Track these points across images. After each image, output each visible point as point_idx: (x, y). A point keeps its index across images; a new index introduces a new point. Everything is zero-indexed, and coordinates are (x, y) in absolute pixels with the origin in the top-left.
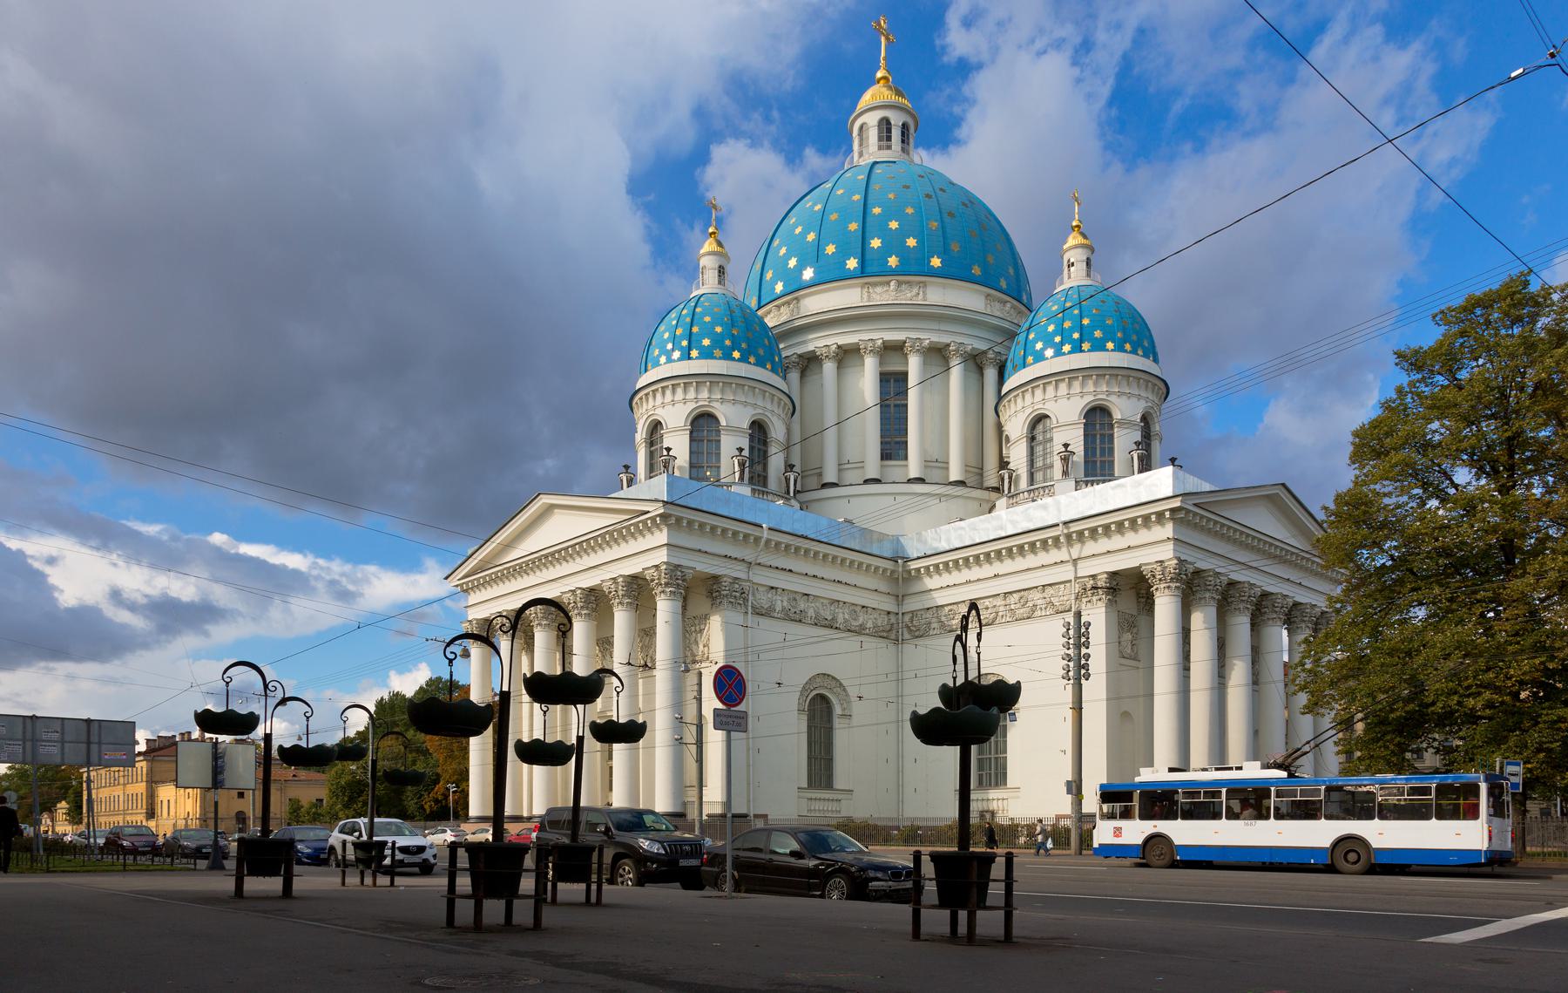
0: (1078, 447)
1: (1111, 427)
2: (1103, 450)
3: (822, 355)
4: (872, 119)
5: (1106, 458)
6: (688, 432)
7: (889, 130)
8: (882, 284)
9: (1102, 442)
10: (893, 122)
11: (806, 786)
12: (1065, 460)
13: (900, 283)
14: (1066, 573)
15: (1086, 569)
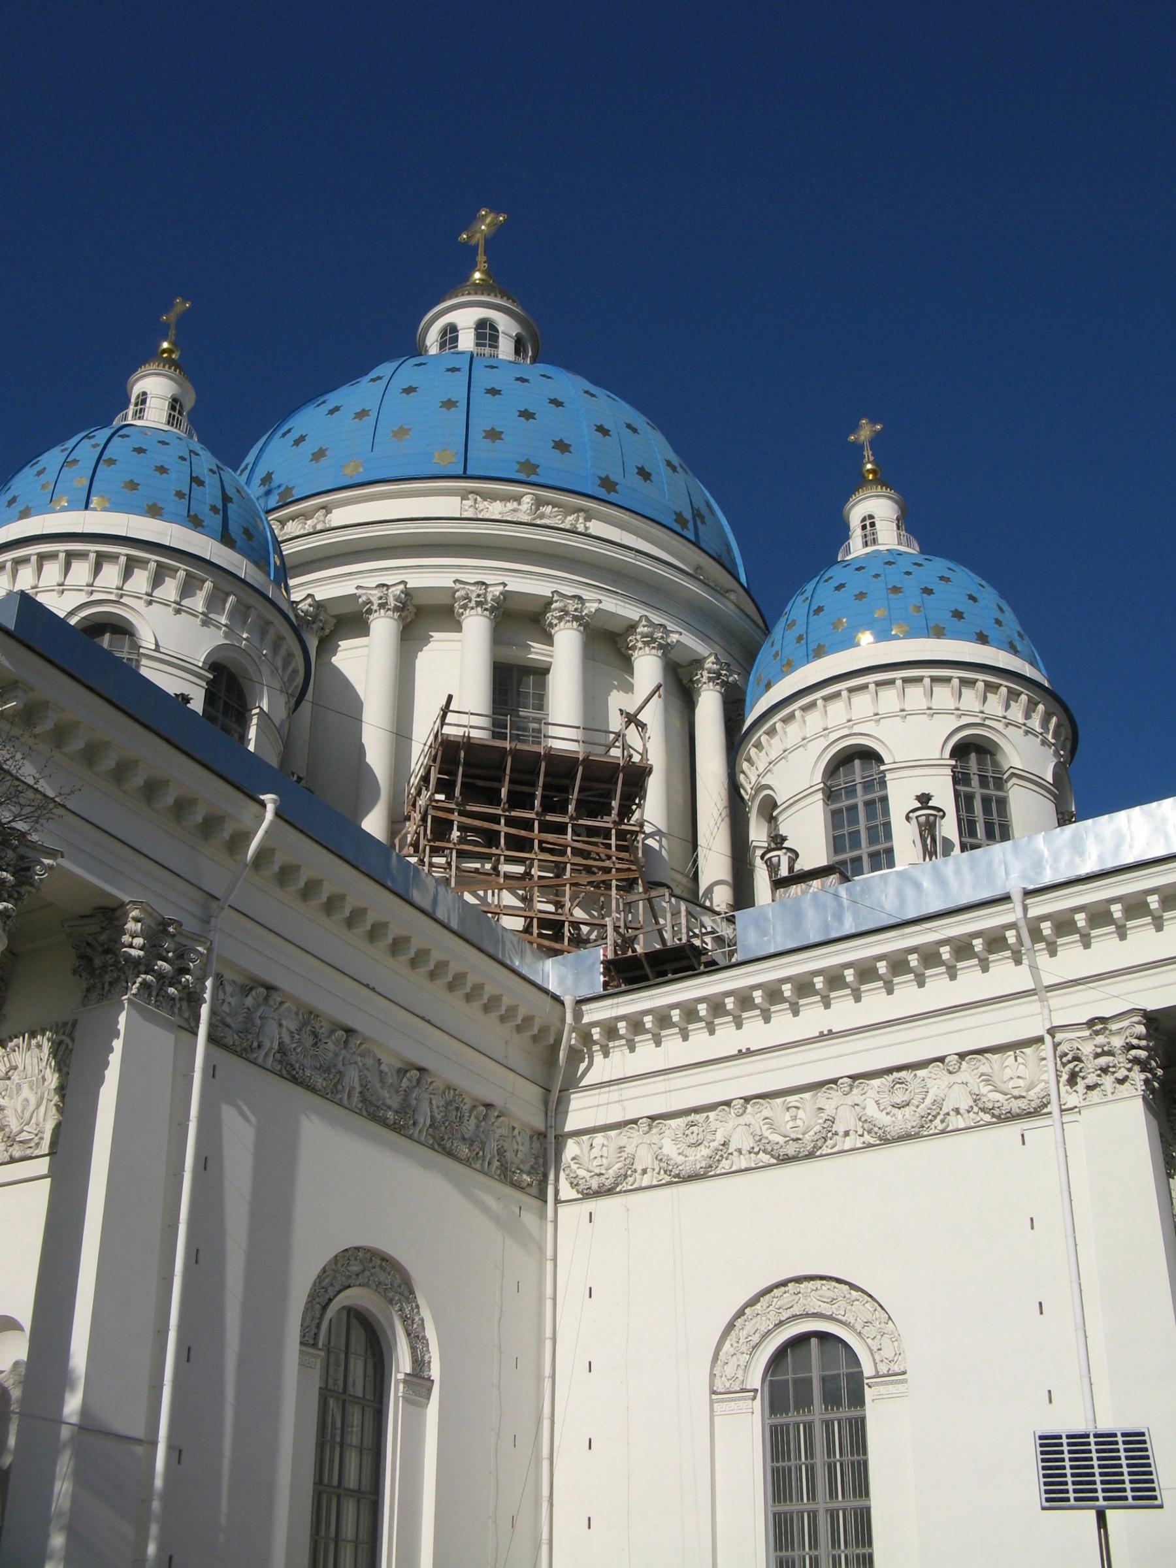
1: (1000, 784)
9: (987, 810)
12: (928, 829)
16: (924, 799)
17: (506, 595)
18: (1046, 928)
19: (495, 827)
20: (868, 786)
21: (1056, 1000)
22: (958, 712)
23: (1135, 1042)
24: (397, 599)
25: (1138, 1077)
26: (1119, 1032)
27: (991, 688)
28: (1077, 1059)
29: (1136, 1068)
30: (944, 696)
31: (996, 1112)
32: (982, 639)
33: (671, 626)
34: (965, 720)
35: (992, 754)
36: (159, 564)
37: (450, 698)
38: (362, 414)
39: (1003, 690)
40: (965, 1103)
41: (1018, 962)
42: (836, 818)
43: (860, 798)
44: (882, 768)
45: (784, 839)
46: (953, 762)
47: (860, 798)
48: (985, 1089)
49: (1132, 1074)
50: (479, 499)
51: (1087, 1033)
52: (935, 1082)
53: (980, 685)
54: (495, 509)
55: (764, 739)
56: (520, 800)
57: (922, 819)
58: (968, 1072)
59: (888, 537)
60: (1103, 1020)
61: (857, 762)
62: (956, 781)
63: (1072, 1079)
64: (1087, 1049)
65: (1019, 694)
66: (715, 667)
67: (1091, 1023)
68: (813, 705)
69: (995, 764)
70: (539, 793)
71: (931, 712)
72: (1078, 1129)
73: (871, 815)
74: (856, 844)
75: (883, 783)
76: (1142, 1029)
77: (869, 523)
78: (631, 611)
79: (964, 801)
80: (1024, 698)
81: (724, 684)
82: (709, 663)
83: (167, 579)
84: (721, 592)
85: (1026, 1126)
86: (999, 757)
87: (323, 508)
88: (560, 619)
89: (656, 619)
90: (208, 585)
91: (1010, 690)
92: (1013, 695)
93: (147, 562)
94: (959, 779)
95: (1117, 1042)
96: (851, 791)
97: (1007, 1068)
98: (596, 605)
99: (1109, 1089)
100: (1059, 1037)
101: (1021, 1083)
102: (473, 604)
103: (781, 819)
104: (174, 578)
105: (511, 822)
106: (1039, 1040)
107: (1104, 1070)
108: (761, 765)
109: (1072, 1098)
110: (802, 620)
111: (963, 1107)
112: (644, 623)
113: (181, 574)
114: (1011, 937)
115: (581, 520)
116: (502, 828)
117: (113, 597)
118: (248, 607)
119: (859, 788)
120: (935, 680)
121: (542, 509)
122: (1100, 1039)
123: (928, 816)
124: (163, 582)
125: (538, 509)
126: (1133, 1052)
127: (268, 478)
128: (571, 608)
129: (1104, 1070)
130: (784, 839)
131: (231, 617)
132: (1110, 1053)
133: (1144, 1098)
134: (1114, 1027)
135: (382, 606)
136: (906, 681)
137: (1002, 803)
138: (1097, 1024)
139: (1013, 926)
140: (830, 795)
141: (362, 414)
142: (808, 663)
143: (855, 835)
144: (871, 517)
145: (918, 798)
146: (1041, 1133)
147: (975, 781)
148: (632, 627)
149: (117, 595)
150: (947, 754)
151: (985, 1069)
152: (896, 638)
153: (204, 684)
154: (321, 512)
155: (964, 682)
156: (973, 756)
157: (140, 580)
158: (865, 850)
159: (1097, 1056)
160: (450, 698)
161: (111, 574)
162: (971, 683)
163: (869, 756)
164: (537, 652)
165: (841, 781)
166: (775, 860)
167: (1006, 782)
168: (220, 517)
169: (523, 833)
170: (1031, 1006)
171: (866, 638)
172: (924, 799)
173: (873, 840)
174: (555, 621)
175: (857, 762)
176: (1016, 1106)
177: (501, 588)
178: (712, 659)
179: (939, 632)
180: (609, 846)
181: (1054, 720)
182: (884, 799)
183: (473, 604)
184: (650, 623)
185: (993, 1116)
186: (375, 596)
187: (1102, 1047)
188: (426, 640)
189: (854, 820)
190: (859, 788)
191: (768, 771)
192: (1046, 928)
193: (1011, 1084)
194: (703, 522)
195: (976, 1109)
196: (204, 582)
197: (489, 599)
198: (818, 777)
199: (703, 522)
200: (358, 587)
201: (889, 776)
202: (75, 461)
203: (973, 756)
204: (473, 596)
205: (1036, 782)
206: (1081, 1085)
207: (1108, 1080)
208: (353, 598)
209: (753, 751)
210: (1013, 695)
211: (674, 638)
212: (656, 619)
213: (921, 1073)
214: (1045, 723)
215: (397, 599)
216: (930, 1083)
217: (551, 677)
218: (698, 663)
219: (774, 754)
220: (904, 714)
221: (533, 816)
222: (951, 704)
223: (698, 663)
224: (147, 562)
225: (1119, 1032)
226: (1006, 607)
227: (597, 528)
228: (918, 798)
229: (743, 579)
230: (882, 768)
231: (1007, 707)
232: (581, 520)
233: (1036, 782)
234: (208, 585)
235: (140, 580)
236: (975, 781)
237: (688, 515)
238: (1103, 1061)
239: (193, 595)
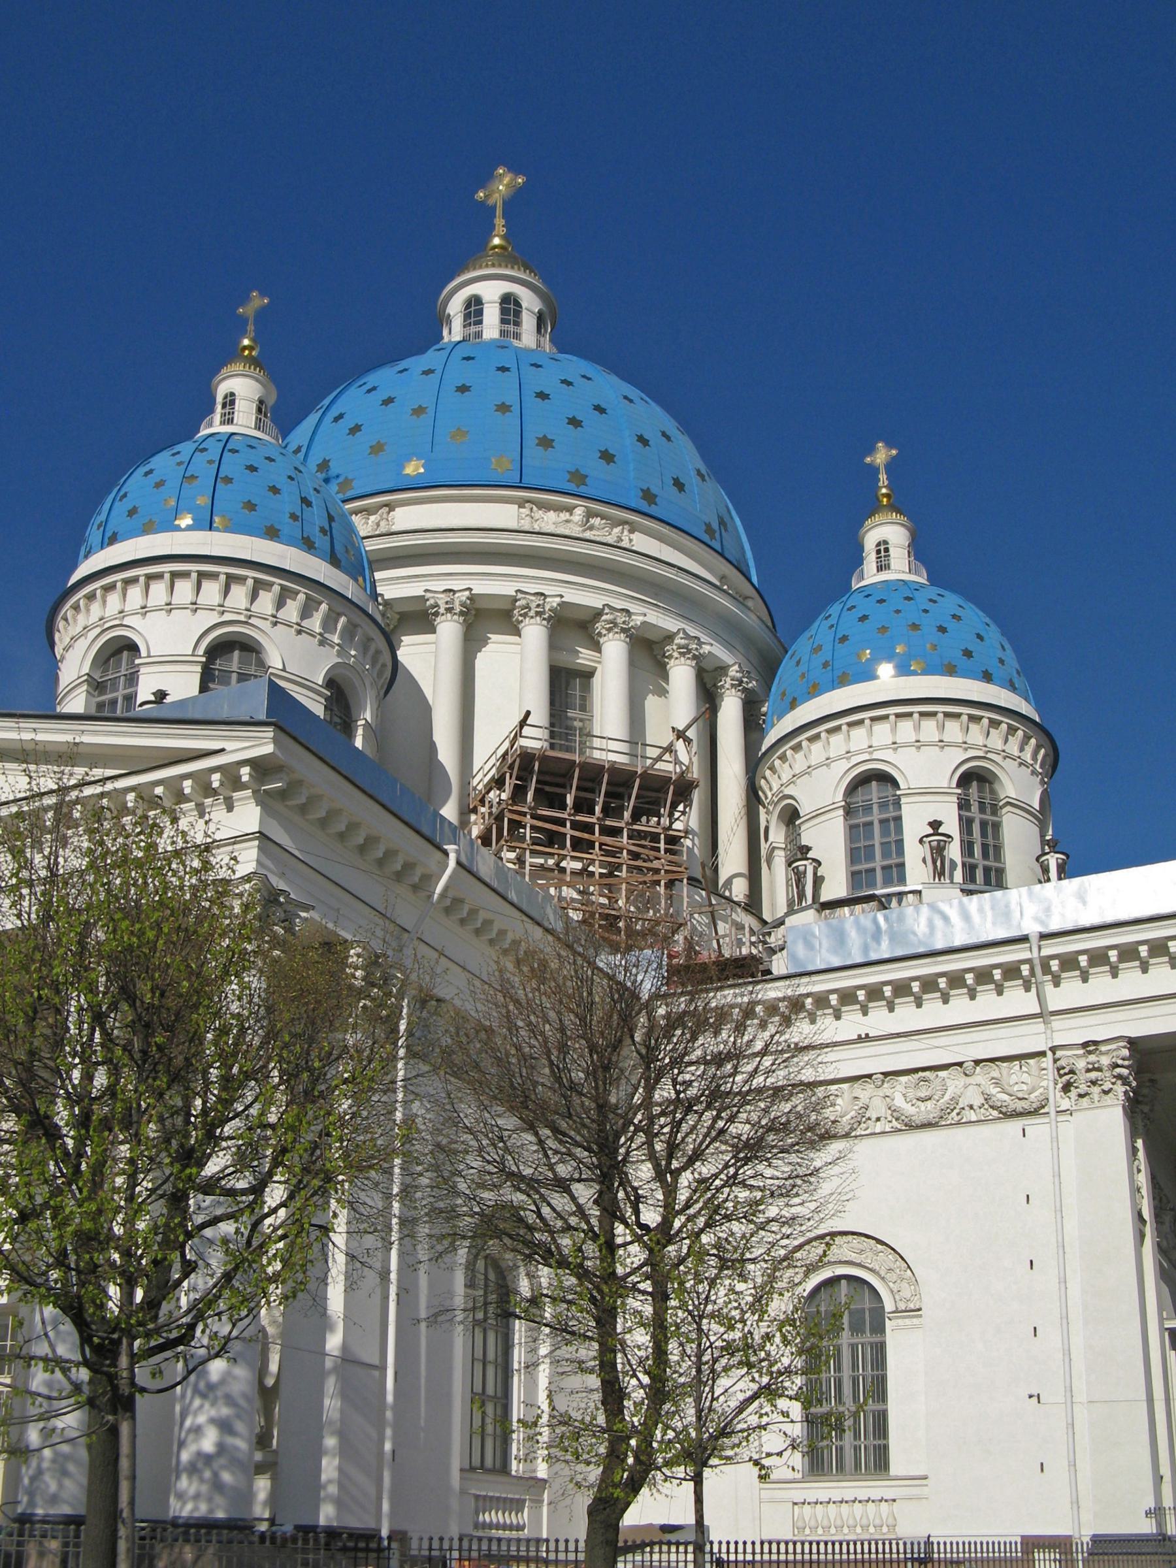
0: (951, 826)
1: (995, 809)
2: (985, 847)
3: (437, 605)
4: (491, 292)
5: (991, 863)
6: (199, 669)
7: (518, 314)
8: (559, 508)
9: (984, 834)
10: (524, 305)
12: (938, 851)
13: (590, 514)
14: (1032, 1038)
15: (1072, 1032)
16: (935, 825)
17: (563, 605)
18: (1055, 965)
19: (561, 829)
20: (883, 806)
21: (1057, 1023)
23: (1120, 1062)
24: (463, 605)
25: (1120, 1089)
26: (1107, 1053)
27: (994, 724)
28: (1072, 1072)
29: (1119, 1082)
30: (953, 731)
31: (1004, 1110)
32: (987, 677)
33: (704, 638)
34: (972, 753)
35: (991, 783)
36: (283, 588)
37: (528, 713)
38: (419, 411)
39: (1004, 727)
40: (978, 1101)
41: (1028, 989)
42: (853, 832)
43: (876, 816)
44: (898, 793)
45: (809, 849)
46: (959, 791)
47: (876, 816)
48: (994, 1090)
49: (1115, 1087)
50: (535, 508)
51: (1081, 1052)
52: (954, 1083)
53: (985, 722)
54: (549, 521)
55: (789, 753)
56: (584, 806)
57: (934, 844)
58: (981, 1076)
59: (900, 567)
60: (1095, 1043)
61: (874, 783)
62: (960, 807)
63: (1067, 1088)
64: (1081, 1064)
65: (1017, 729)
66: (739, 675)
67: (1085, 1045)
68: (838, 729)
69: (993, 792)
70: (600, 800)
71: (942, 744)
72: (1069, 1128)
73: (885, 832)
74: (870, 857)
75: (897, 804)
76: (1126, 1052)
77: (883, 549)
78: (669, 623)
79: (966, 824)
80: (1020, 733)
81: (745, 690)
82: (733, 671)
83: (288, 601)
84: (740, 599)
85: (1026, 1122)
86: (996, 786)
87: (386, 505)
88: (609, 630)
89: (692, 632)
90: (324, 607)
91: (1010, 726)
92: (1012, 730)
93: (271, 584)
94: (963, 805)
95: (1105, 1061)
96: (868, 809)
97: (1015, 1075)
98: (641, 618)
99: (1096, 1097)
100: (1059, 1054)
101: (1025, 1087)
102: (532, 613)
103: (803, 828)
104: (294, 599)
105: (576, 826)
106: (1043, 1054)
107: (1094, 1083)
108: (786, 775)
109: (1065, 1104)
110: (827, 647)
111: (976, 1104)
112: (681, 635)
113: (301, 597)
114: (1025, 970)
115: (626, 533)
116: (568, 830)
117: (242, 618)
118: (356, 626)
119: (875, 807)
120: (947, 715)
121: (592, 521)
122: (1092, 1058)
123: (939, 841)
124: (285, 604)
125: (588, 521)
126: (1118, 1070)
127: (324, 466)
128: (619, 621)
129: (1094, 1083)
130: (809, 849)
131: (341, 637)
132: (1099, 1069)
133: (1124, 1106)
134: (1103, 1048)
135: (449, 610)
136: (922, 714)
137: (997, 826)
138: (1090, 1046)
139: (1028, 961)
141: (419, 411)
142: (834, 689)
144: (885, 542)
145: (931, 824)
146: (1038, 1128)
147: (975, 808)
148: (670, 637)
149: (246, 616)
151: (995, 1074)
152: (914, 673)
153: (323, 701)
154: (386, 509)
155: (972, 718)
156: (975, 784)
157: (265, 603)
158: (878, 862)
159: (1088, 1071)
160: (528, 713)
161: (239, 596)
162: (978, 719)
164: (585, 657)
165: (859, 798)
167: (1001, 808)
168: (328, 538)
169: (586, 836)
170: (1038, 1026)
171: (886, 670)
172: (935, 825)
173: (886, 854)
174: (604, 632)
175: (874, 783)
176: (1020, 1106)
177: (558, 600)
178: (736, 667)
179: (950, 670)
180: (658, 850)
182: (898, 819)
183: (532, 613)
184: (687, 636)
185: (1001, 1112)
186: (442, 599)
187: (1093, 1064)
188: (485, 642)
190: (875, 807)
191: (791, 782)
192: (1055, 965)
193: (1016, 1088)
194: (726, 530)
195: (986, 1106)
196: (320, 603)
197: (547, 607)
198: (839, 796)
199: (726, 530)
200: (427, 591)
201: (903, 800)
202: (193, 477)
203: (975, 784)
204: (533, 605)
205: (1026, 809)
206: (1073, 1093)
207: (1096, 1090)
208: (422, 599)
209: (777, 763)
210: (1012, 730)
211: (706, 649)
212: (692, 632)
213: (942, 1074)
215: (463, 605)
216: (949, 1082)
217: (596, 681)
218: (723, 669)
219: (798, 769)
220: (918, 744)
221: (594, 820)
223: (723, 669)
224: (271, 584)
225: (1107, 1053)
226: (1007, 646)
227: (641, 542)
228: (931, 824)
229: (755, 579)
230: (898, 793)
231: (1006, 741)
232: (626, 533)
233: (1026, 809)
234: (324, 607)
235: (265, 603)
236: (975, 808)
237: (715, 526)
238: (1093, 1075)
239: (311, 616)
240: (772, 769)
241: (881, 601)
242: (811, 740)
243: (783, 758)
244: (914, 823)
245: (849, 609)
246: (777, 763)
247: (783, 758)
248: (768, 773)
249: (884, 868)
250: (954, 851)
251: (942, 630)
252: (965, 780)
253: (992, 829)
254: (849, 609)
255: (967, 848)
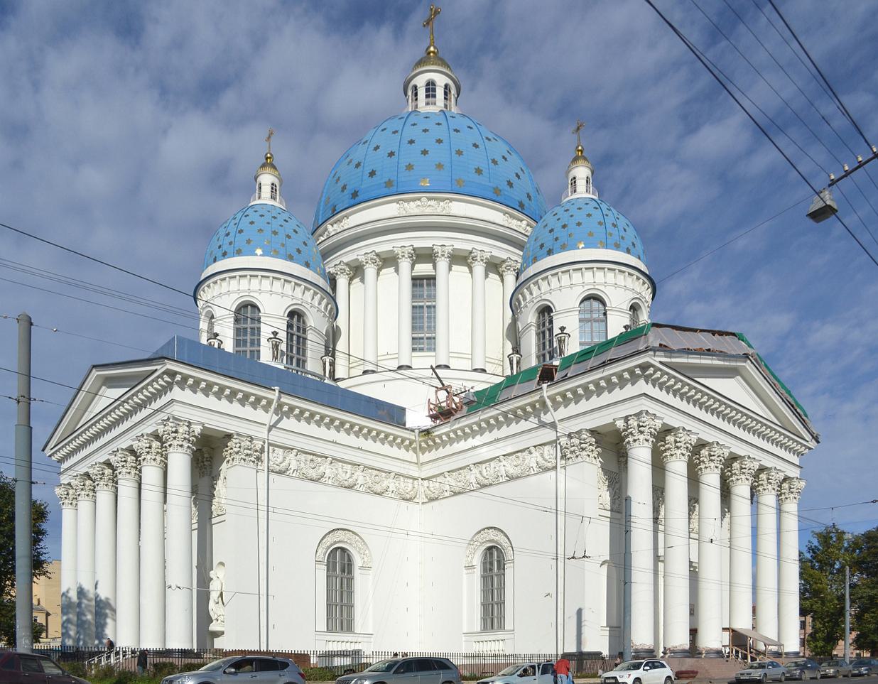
1: (305, 331)
2: (298, 349)
5: (300, 357)
9: (298, 343)
11: (326, 630)
22: (293, 297)
34: (295, 302)
39: (312, 291)
42: (238, 332)
65: (317, 294)
69: (304, 322)
73: (253, 334)
79: (290, 336)
86: (305, 318)
91: (315, 292)
94: (290, 326)
140: (237, 320)
143: (245, 341)
147: (295, 329)
150: (286, 315)
156: (296, 316)
163: (254, 306)
166: (212, 343)
179: (290, 258)
181: (330, 306)
189: (245, 334)
205: (318, 332)
209: (206, 288)
214: (326, 308)
222: (290, 293)
233: (318, 332)
236: (295, 329)
240: (204, 291)
241: (262, 216)
242: (222, 280)
243: (209, 286)
244: (266, 331)
245: (246, 216)
246: (206, 288)
247: (209, 286)
248: (202, 292)
249: (251, 351)
250: (283, 347)
251: (289, 237)
252: (292, 314)
253: (302, 341)
254: (246, 216)
255: (290, 347)
